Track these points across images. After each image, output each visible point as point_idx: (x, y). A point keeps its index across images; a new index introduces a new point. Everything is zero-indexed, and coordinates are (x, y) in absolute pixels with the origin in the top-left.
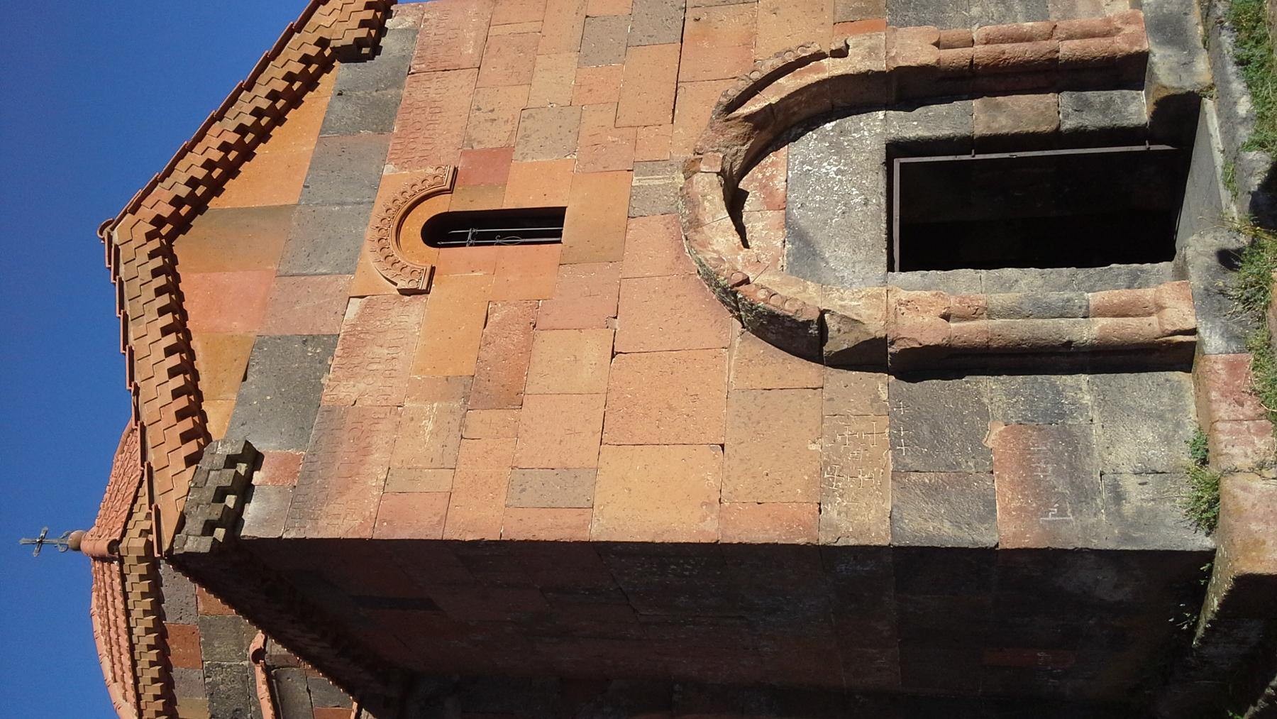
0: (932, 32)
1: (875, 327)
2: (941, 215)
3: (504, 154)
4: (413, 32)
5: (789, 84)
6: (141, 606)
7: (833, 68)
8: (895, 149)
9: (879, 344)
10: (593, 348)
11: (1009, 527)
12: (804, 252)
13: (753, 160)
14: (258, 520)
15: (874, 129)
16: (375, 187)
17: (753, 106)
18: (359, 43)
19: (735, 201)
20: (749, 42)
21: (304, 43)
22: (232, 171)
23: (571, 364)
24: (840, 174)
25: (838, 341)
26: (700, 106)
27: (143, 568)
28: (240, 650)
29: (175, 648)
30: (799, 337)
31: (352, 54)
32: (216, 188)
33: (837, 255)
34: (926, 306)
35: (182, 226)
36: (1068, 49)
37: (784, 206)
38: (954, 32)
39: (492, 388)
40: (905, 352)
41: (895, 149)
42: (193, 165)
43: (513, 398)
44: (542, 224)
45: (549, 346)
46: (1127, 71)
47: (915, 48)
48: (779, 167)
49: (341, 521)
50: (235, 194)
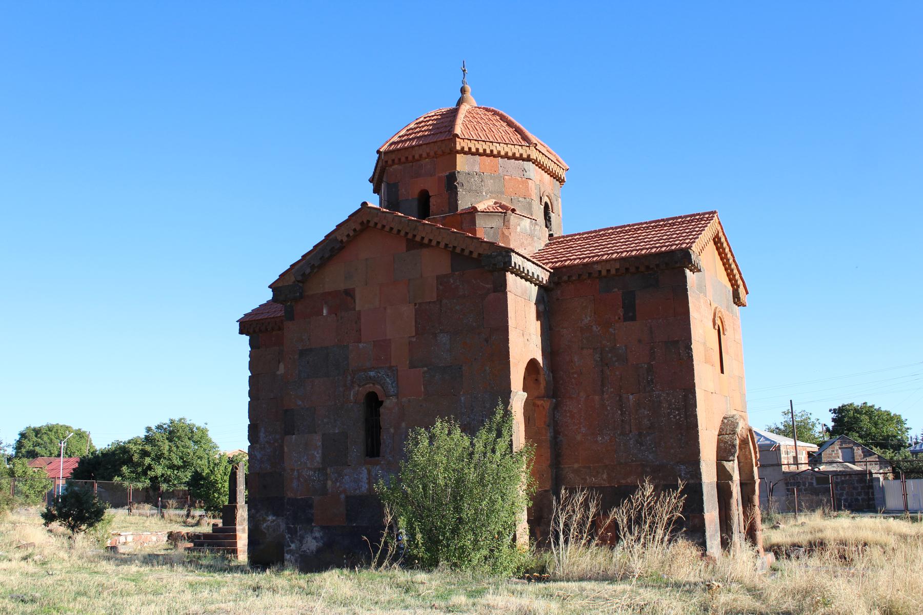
3: (727, 353)
6: (510, 150)
18: (739, 299)
27: (525, 156)
28: (491, 193)
40: (729, 487)
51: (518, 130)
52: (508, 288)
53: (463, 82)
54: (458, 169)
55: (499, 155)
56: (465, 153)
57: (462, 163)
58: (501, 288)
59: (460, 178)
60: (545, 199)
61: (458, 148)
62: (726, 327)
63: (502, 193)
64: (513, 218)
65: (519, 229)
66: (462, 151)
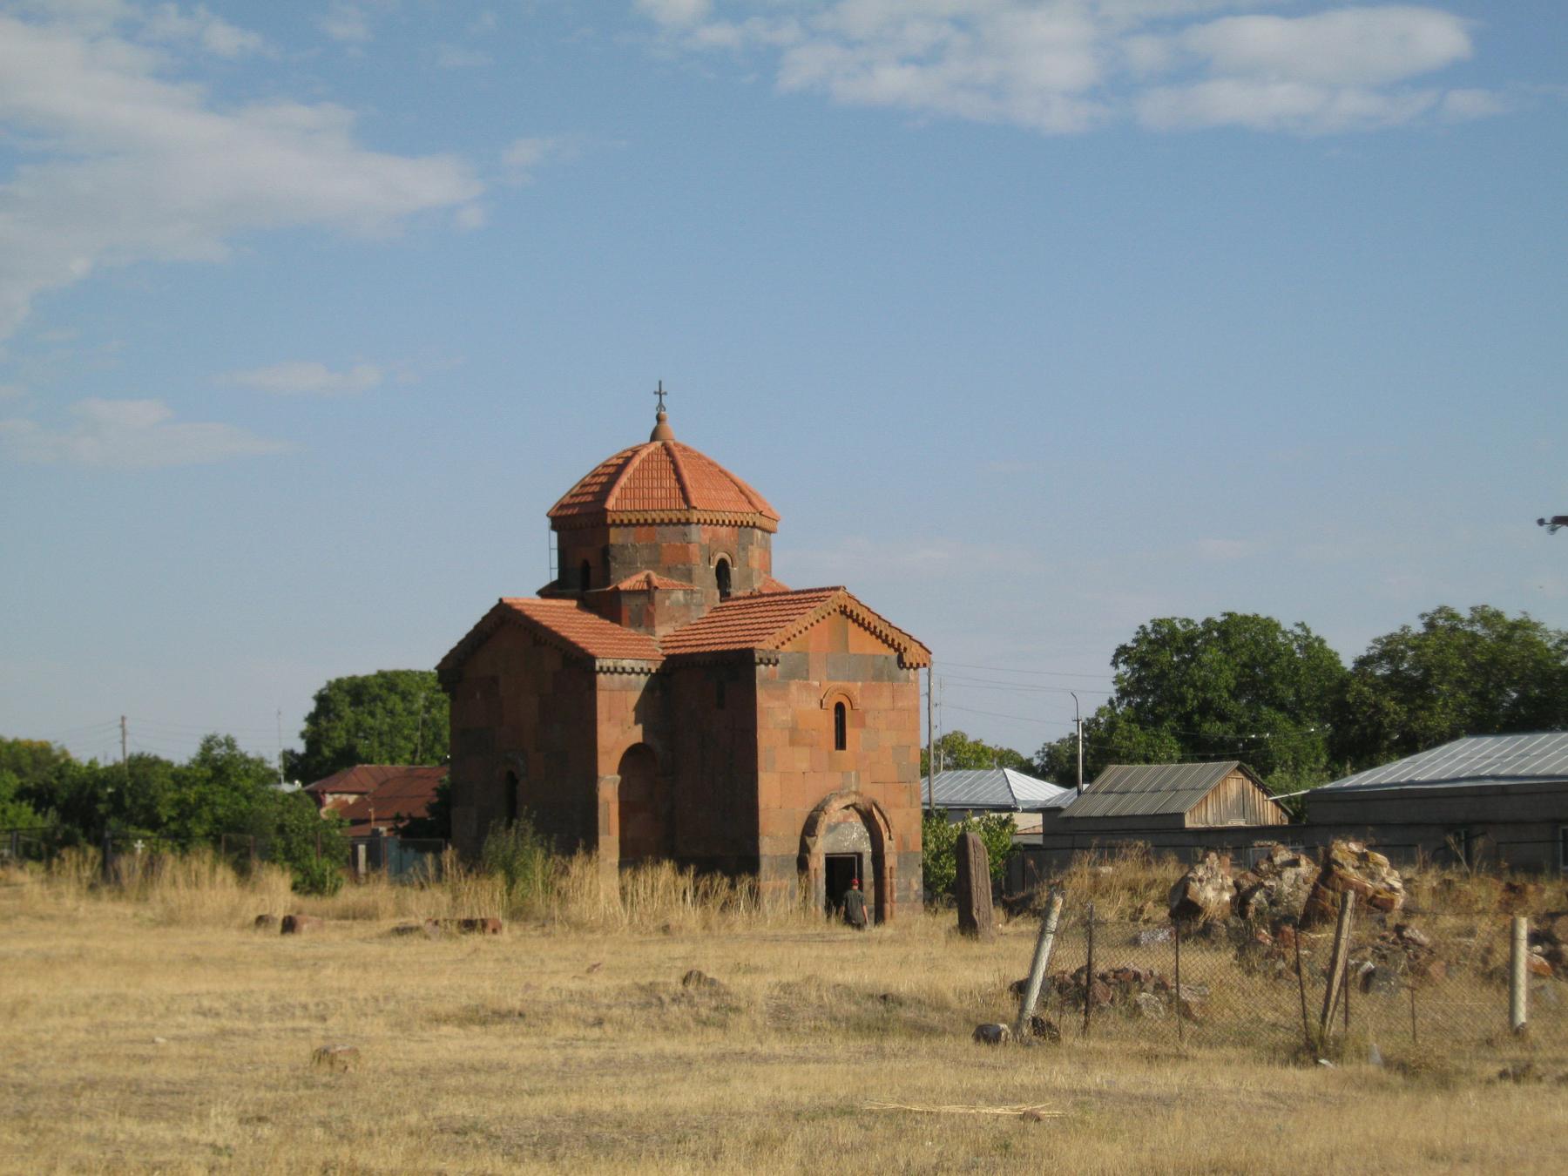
0: (895, 866)
1: (814, 850)
2: (842, 871)
3: (862, 724)
4: (908, 679)
5: (881, 822)
6: (665, 516)
7: (886, 836)
8: (860, 855)
9: (809, 851)
10: (804, 766)
12: (832, 829)
13: (859, 811)
14: (761, 669)
15: (866, 848)
16: (855, 680)
17: (875, 811)
19: (847, 807)
20: (897, 806)
21: (905, 643)
22: (861, 625)
23: (801, 759)
24: (854, 838)
25: (809, 841)
29: (644, 529)
31: (900, 660)
32: (856, 621)
33: (831, 838)
34: (818, 863)
35: (843, 612)
36: (887, 906)
37: (845, 821)
38: (895, 873)
39: (795, 736)
41: (860, 855)
42: (863, 614)
43: (793, 742)
44: (841, 743)
47: (890, 861)
48: (856, 821)
50: (853, 627)
51: (683, 489)
52: (599, 686)
53: (661, 405)
54: (612, 540)
55: (654, 523)
56: (618, 526)
57: (616, 537)
58: (592, 686)
59: (613, 551)
60: (719, 556)
61: (609, 521)
62: (859, 702)
63: (659, 562)
64: (658, 596)
65: (667, 603)
66: (614, 524)
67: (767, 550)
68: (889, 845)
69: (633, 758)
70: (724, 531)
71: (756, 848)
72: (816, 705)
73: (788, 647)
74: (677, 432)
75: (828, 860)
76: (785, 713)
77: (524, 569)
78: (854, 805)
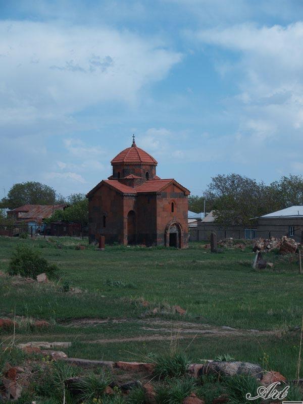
2: (173, 236)
8: (176, 234)
10: (165, 215)
11: (158, 240)
14: (158, 196)
15: (177, 232)
24: (175, 230)
26: (179, 221)
30: (167, 229)
44: (173, 211)
45: (166, 212)
46: (180, 247)
49: (157, 201)
58: (123, 199)
67: (155, 170)
68: (182, 232)
69: (131, 213)
70: (147, 167)
71: (156, 232)
72: (168, 203)
73: (163, 191)
74: (138, 145)
75: (170, 234)
76: (162, 204)
77: (105, 172)
78: (175, 224)
